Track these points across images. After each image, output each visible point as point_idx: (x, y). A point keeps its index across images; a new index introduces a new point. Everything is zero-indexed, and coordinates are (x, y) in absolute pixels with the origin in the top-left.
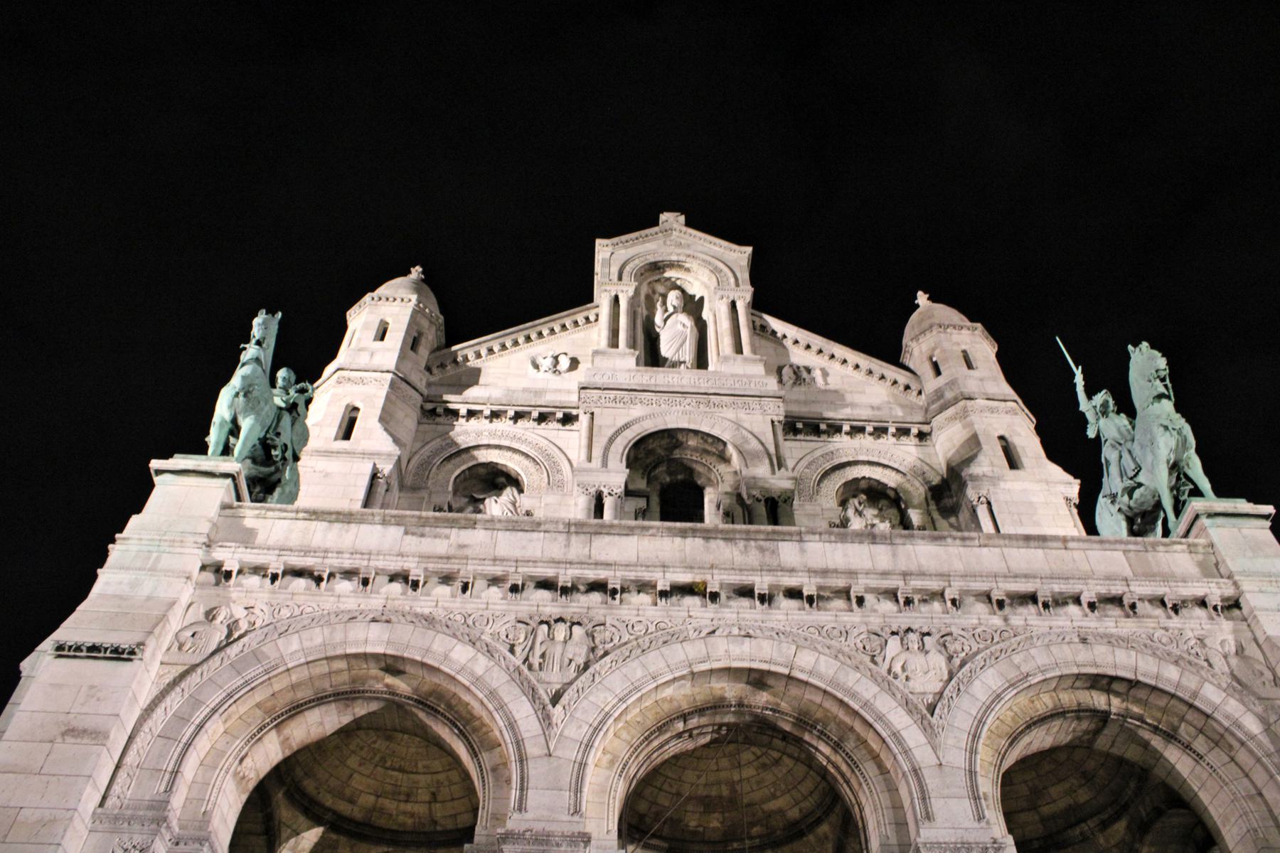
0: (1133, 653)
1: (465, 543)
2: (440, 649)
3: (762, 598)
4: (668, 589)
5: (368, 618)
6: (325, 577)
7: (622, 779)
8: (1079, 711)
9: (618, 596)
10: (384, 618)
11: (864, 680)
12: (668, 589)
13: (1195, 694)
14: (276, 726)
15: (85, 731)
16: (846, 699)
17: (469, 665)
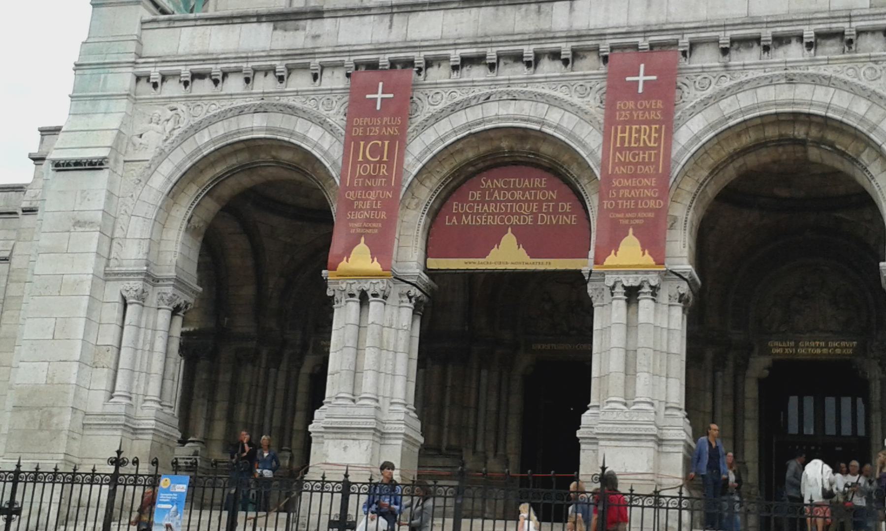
0: (832, 90)
1: (317, 33)
2: (301, 132)
3: (528, 64)
4: (458, 63)
5: (252, 110)
6: (220, 78)
7: (425, 216)
8: (779, 140)
9: (423, 73)
10: (262, 110)
11: (595, 132)
12: (458, 63)
13: (874, 128)
14: (207, 194)
15: (85, 223)
16: (578, 149)
17: (319, 142)
